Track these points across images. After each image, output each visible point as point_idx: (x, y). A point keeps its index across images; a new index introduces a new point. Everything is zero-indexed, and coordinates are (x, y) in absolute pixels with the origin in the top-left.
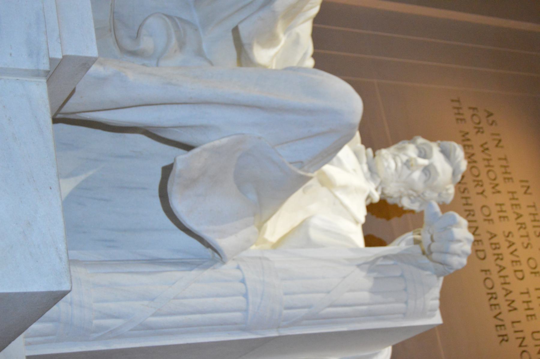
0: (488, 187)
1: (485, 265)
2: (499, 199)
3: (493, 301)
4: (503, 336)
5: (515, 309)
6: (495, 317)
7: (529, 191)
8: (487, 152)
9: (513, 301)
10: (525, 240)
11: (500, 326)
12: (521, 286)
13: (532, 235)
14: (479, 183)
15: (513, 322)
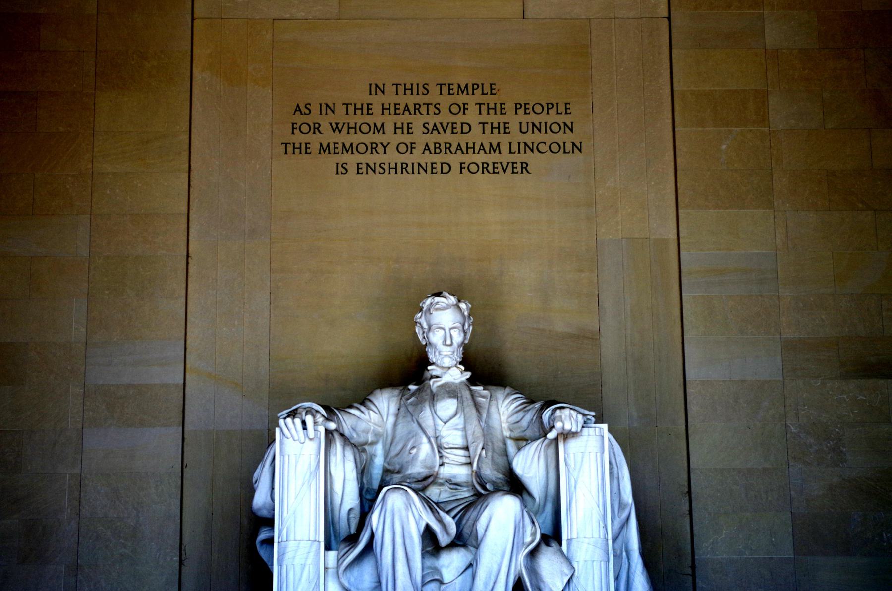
0: (378, 138)
1: (456, 167)
2: (389, 128)
3: (490, 168)
4: (522, 168)
5: (498, 144)
6: (505, 171)
7: (381, 87)
8: (340, 126)
9: (491, 145)
10: (431, 108)
11: (513, 168)
12: (477, 129)
13: (426, 99)
14: (373, 148)
15: (511, 152)
